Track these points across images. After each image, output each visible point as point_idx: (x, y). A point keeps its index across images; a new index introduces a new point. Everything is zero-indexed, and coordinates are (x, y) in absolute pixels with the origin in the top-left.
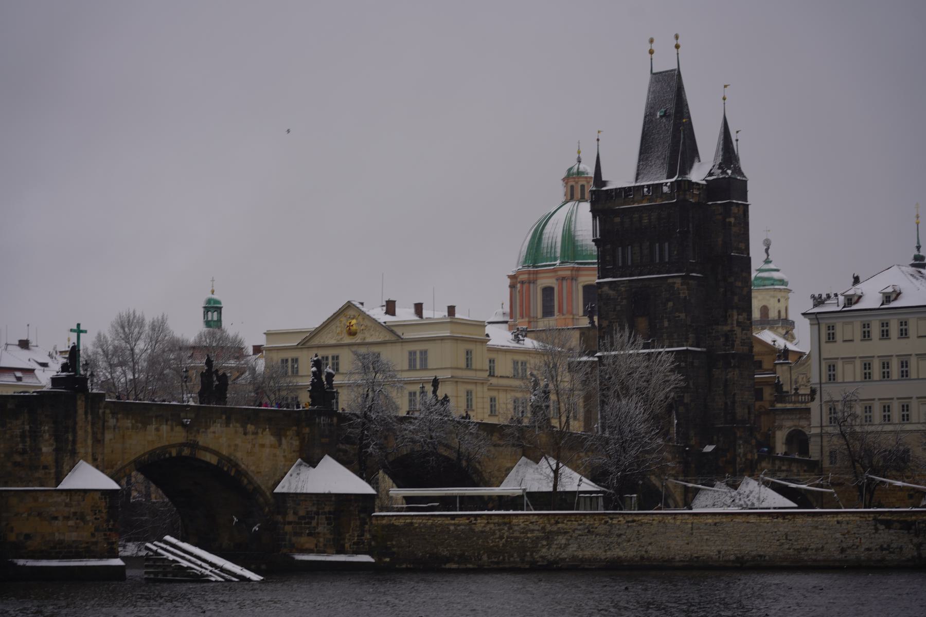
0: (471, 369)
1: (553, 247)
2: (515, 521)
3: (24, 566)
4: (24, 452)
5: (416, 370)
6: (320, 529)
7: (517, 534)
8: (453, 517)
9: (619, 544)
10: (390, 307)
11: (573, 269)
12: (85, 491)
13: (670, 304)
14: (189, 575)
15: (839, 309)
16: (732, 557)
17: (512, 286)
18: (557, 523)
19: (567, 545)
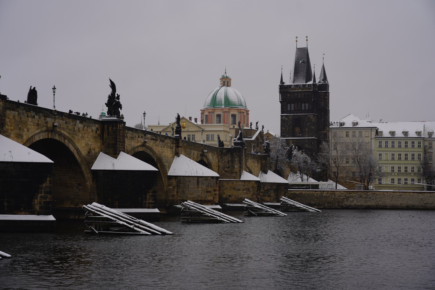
0: (213, 141)
1: (221, 101)
2: (336, 193)
3: (229, 206)
4: (229, 167)
5: (209, 141)
6: (272, 194)
7: (337, 197)
8: (316, 191)
9: (370, 201)
10: (190, 118)
11: (229, 109)
12: (250, 181)
13: (309, 123)
14: (300, 210)
15: (338, 127)
16: (405, 206)
17: (202, 114)
18: (350, 194)
19: (353, 201)
